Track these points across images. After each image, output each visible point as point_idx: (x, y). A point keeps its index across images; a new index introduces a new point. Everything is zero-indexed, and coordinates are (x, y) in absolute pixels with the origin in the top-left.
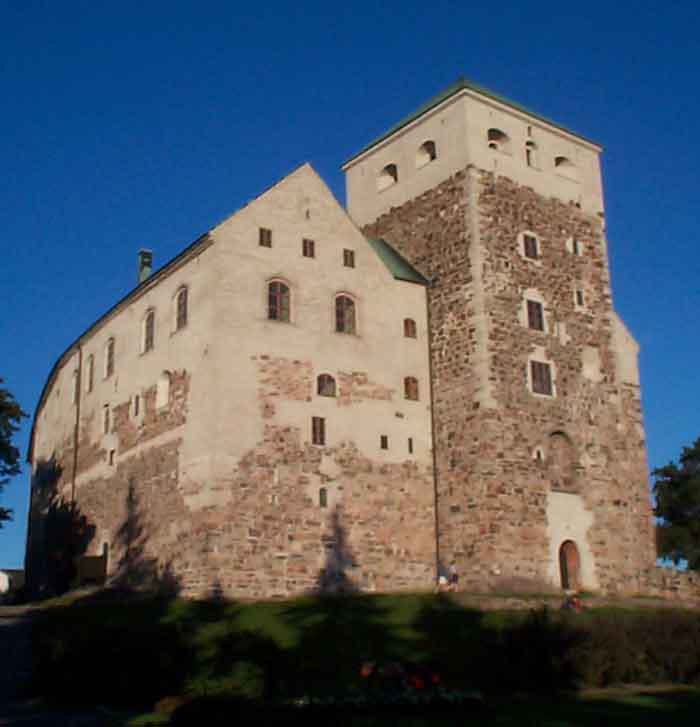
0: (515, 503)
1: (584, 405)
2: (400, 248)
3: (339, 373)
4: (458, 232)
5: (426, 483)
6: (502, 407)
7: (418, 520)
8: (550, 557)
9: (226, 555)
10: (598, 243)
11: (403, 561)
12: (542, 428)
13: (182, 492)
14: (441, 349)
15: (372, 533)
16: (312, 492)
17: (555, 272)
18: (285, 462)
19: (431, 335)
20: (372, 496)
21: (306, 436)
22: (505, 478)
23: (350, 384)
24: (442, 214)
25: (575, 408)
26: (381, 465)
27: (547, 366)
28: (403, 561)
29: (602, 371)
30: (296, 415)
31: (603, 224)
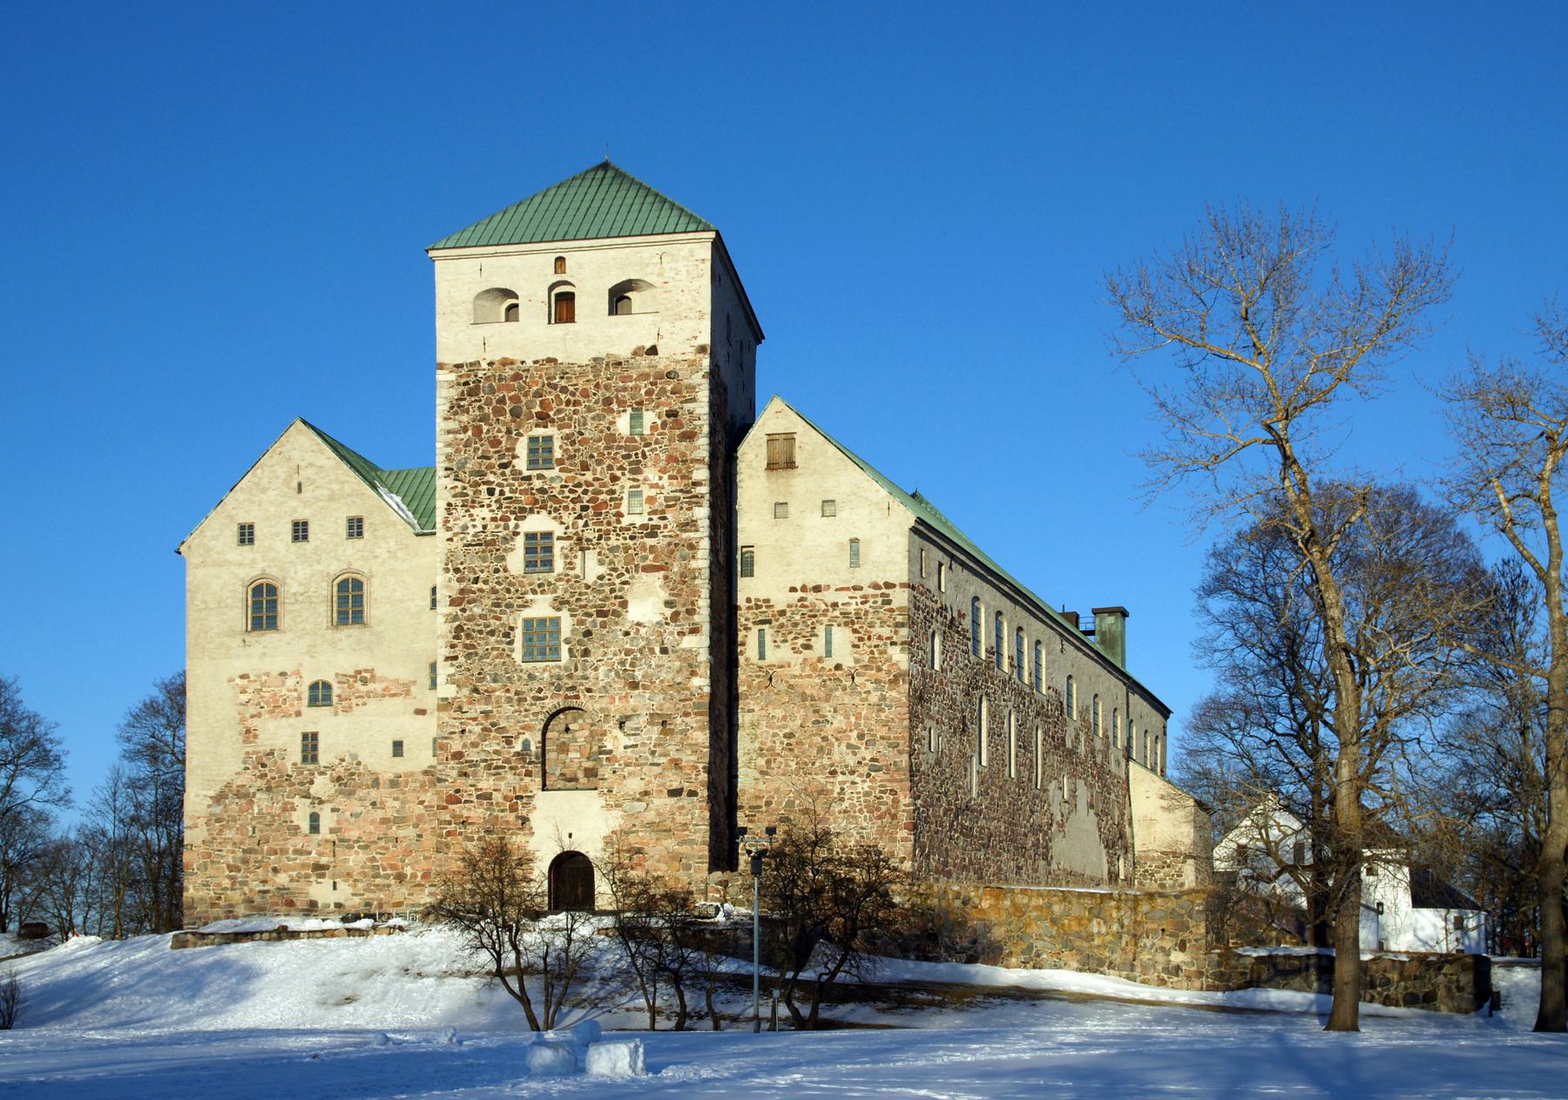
6: (466, 691)
9: (203, 893)
10: (693, 400)
16: (301, 818)
17: (589, 476)
18: (269, 789)
20: (379, 814)
22: (461, 783)
25: (602, 670)
26: (392, 776)
27: (556, 622)
29: (668, 604)
30: (282, 736)
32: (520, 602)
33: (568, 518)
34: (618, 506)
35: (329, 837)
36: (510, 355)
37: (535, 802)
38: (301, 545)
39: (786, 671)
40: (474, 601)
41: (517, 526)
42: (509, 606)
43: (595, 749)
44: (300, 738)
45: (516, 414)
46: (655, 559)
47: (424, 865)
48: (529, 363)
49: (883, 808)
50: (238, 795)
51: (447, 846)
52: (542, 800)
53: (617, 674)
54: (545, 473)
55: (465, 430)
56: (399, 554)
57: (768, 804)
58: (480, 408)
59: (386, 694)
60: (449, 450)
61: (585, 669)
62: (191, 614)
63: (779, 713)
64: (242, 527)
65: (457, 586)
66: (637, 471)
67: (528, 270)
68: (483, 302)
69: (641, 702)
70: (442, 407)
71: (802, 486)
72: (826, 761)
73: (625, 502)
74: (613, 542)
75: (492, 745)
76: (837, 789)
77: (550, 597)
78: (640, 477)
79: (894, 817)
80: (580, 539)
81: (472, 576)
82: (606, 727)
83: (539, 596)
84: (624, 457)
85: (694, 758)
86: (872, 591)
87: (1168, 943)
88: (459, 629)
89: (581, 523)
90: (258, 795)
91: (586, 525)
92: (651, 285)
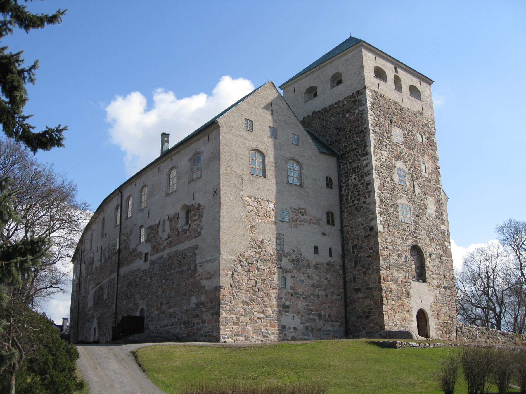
2: (320, 135)
4: (358, 126)
5: (339, 274)
6: (386, 229)
7: (335, 297)
8: (413, 319)
11: (327, 320)
13: (199, 278)
14: (348, 195)
15: (310, 304)
17: (412, 152)
19: (340, 188)
20: (311, 282)
24: (348, 115)
28: (327, 320)
29: (436, 211)
35: (290, 291)
59: (310, 222)
66: (423, 156)
88: (382, 201)
89: (412, 169)
91: (413, 171)
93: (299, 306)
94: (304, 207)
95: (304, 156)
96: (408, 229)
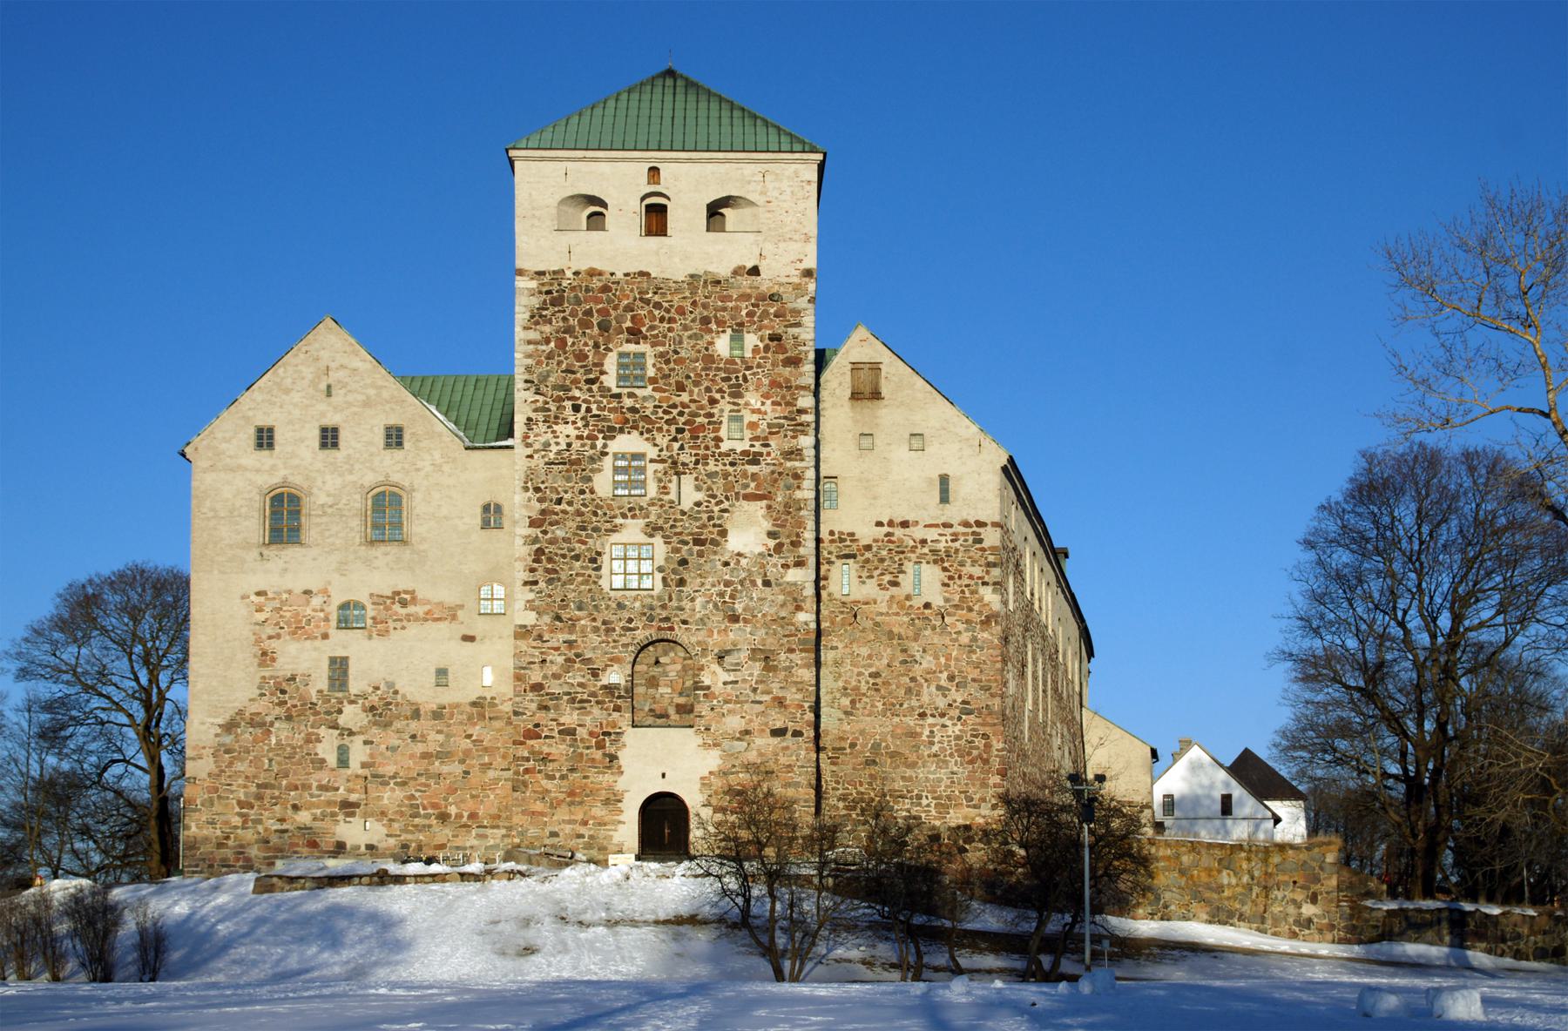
0: (558, 749)
1: (721, 595)
3: (372, 595)
6: (547, 619)
7: (491, 774)
8: (621, 818)
9: (207, 831)
10: (798, 325)
11: (465, 826)
12: (624, 640)
16: (327, 749)
17: (685, 397)
18: (289, 718)
20: (419, 748)
21: (321, 681)
22: (541, 717)
23: (387, 609)
25: (699, 601)
28: (465, 826)
29: (771, 535)
30: (305, 660)
31: (812, 287)
32: (608, 526)
33: (663, 441)
34: (718, 430)
35: (360, 772)
36: (598, 266)
37: (624, 738)
38: (330, 454)
39: (872, 607)
40: (557, 523)
41: (605, 446)
42: (596, 529)
43: (689, 683)
44: (325, 664)
45: (604, 327)
46: (757, 487)
47: (470, 804)
48: (619, 275)
49: (975, 753)
50: (252, 723)
51: (525, 784)
52: (631, 736)
53: (716, 605)
54: (637, 391)
55: (547, 341)
56: (446, 468)
57: (853, 745)
58: (565, 319)
59: (428, 617)
60: (530, 361)
61: (680, 600)
62: (197, 523)
63: (864, 651)
64: (260, 430)
65: (538, 506)
66: (739, 395)
67: (620, 178)
68: (564, 208)
69: (741, 636)
70: (521, 316)
71: (887, 415)
72: (914, 703)
73: (724, 427)
74: (711, 467)
75: (575, 677)
76: (927, 732)
77: (641, 522)
78: (740, 401)
79: (986, 762)
80: (675, 463)
81: (555, 497)
82: (703, 661)
83: (629, 521)
84: (724, 380)
85: (799, 696)
86: (962, 529)
87: (1299, 896)
88: (540, 552)
89: (676, 445)
90: (277, 725)
91: (682, 448)
92: (752, 204)
93: (386, 801)
94: (409, 586)
95: (418, 470)
96: (637, 604)
